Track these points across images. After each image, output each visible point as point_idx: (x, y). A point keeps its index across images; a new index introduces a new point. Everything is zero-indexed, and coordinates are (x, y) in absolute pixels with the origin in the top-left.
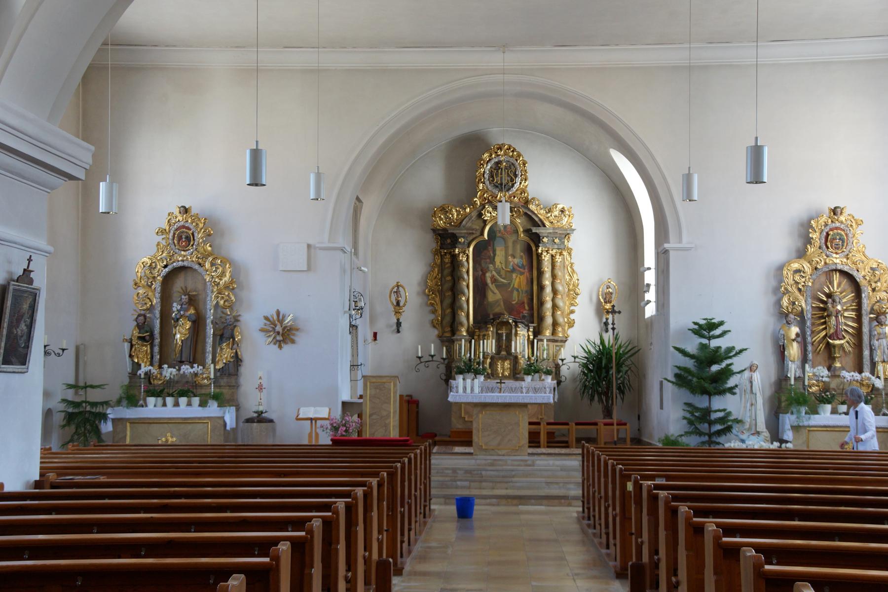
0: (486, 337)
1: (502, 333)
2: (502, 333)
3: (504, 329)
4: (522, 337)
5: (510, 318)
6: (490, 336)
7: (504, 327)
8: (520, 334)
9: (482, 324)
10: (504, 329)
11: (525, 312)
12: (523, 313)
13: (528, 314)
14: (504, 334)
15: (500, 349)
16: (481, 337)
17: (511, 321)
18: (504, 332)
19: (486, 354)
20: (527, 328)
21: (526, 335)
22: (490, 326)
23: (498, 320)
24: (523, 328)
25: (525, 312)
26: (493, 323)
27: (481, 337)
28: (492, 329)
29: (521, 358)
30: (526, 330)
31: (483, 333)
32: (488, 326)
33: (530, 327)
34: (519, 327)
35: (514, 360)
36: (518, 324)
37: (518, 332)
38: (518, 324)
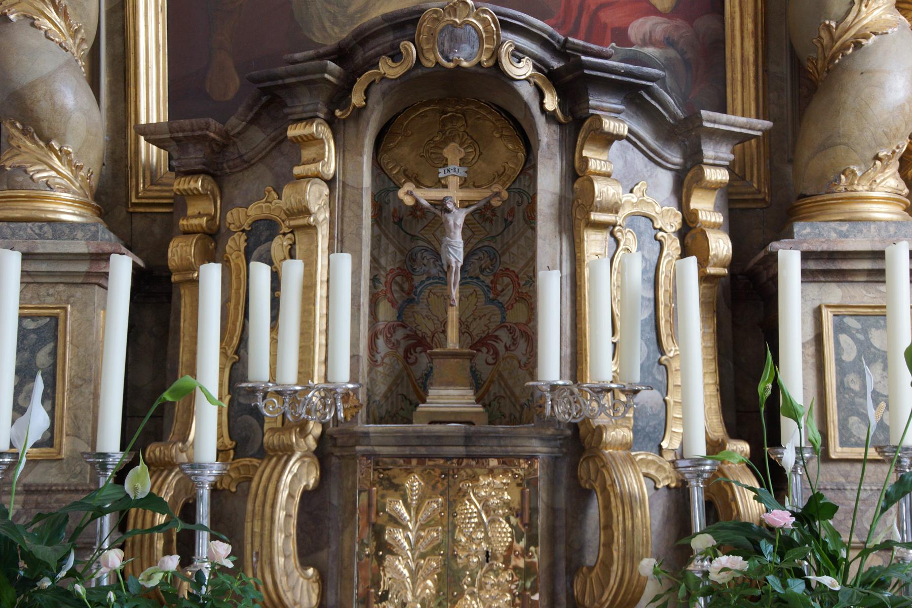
0: (279, 245)
1: (441, 205)
2: (441, 205)
3: (453, 173)
4: (628, 239)
5: (511, 40)
6: (311, 229)
7: (453, 153)
8: (614, 208)
9: (235, 123)
10: (453, 173)
11: (639, 28)
12: (621, 37)
13: (668, 42)
14: (457, 219)
15: (424, 360)
16: (236, 244)
17: (522, 70)
18: (454, 194)
19: (270, 409)
20: (675, 157)
21: (671, 221)
22: (320, 129)
23: (396, 56)
24: (638, 159)
25: (639, 28)
26: (341, 94)
27: (236, 244)
28: (330, 166)
29: (628, 446)
30: (665, 179)
31: (255, 211)
32: (293, 132)
33: (709, 152)
34: (607, 140)
35: (553, 462)
36: (599, 102)
37: (604, 190)
38: (599, 102)
